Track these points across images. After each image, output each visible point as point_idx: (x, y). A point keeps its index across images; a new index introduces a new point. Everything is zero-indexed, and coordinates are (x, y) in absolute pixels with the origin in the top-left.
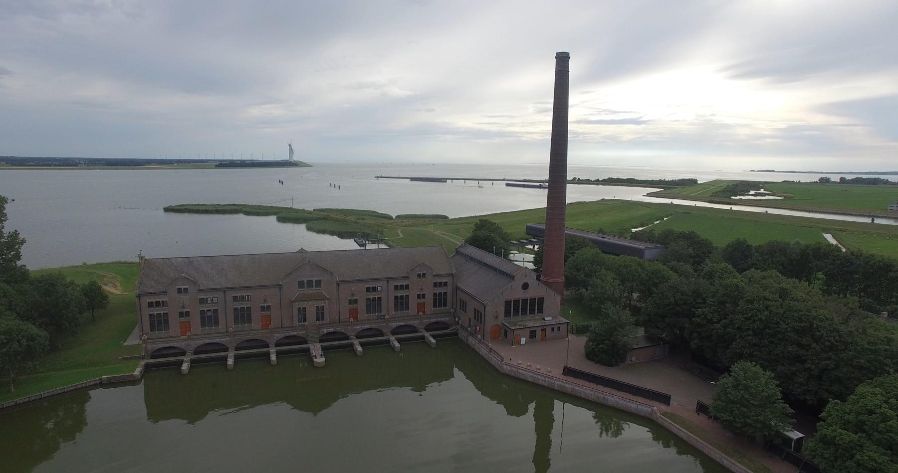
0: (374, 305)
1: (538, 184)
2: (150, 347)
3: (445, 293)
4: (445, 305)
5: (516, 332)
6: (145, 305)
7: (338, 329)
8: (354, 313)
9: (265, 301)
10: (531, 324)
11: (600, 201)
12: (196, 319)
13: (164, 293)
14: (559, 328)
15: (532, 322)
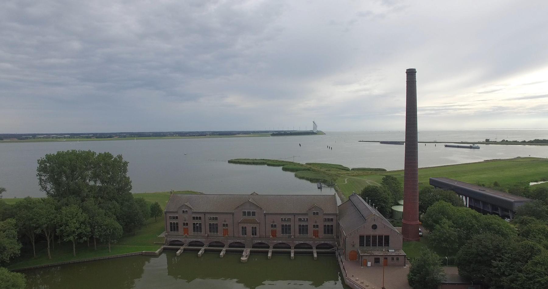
0: (286, 229)
1: (469, 145)
2: (168, 239)
3: (332, 226)
4: (332, 233)
5: (364, 258)
6: (168, 218)
7: (263, 241)
8: (274, 233)
9: (225, 221)
10: (376, 253)
11: (515, 159)
12: (191, 227)
13: (177, 212)
14: (398, 259)
15: (378, 252)
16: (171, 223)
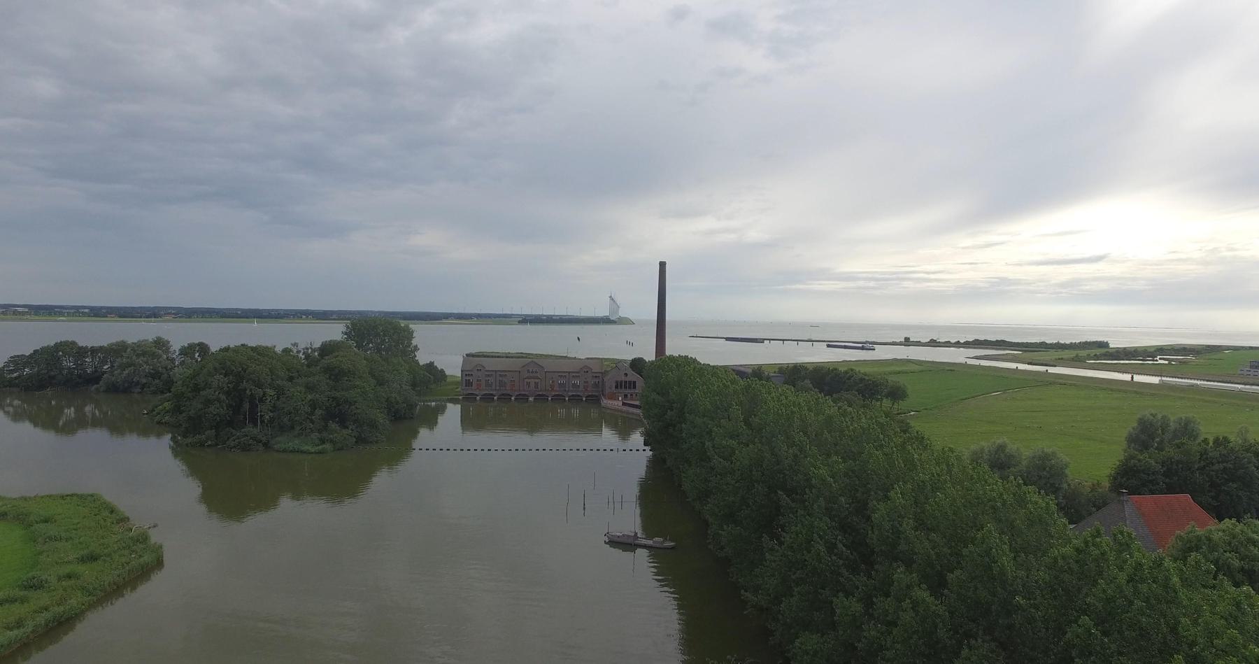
1: (860, 345)
16: (466, 380)
